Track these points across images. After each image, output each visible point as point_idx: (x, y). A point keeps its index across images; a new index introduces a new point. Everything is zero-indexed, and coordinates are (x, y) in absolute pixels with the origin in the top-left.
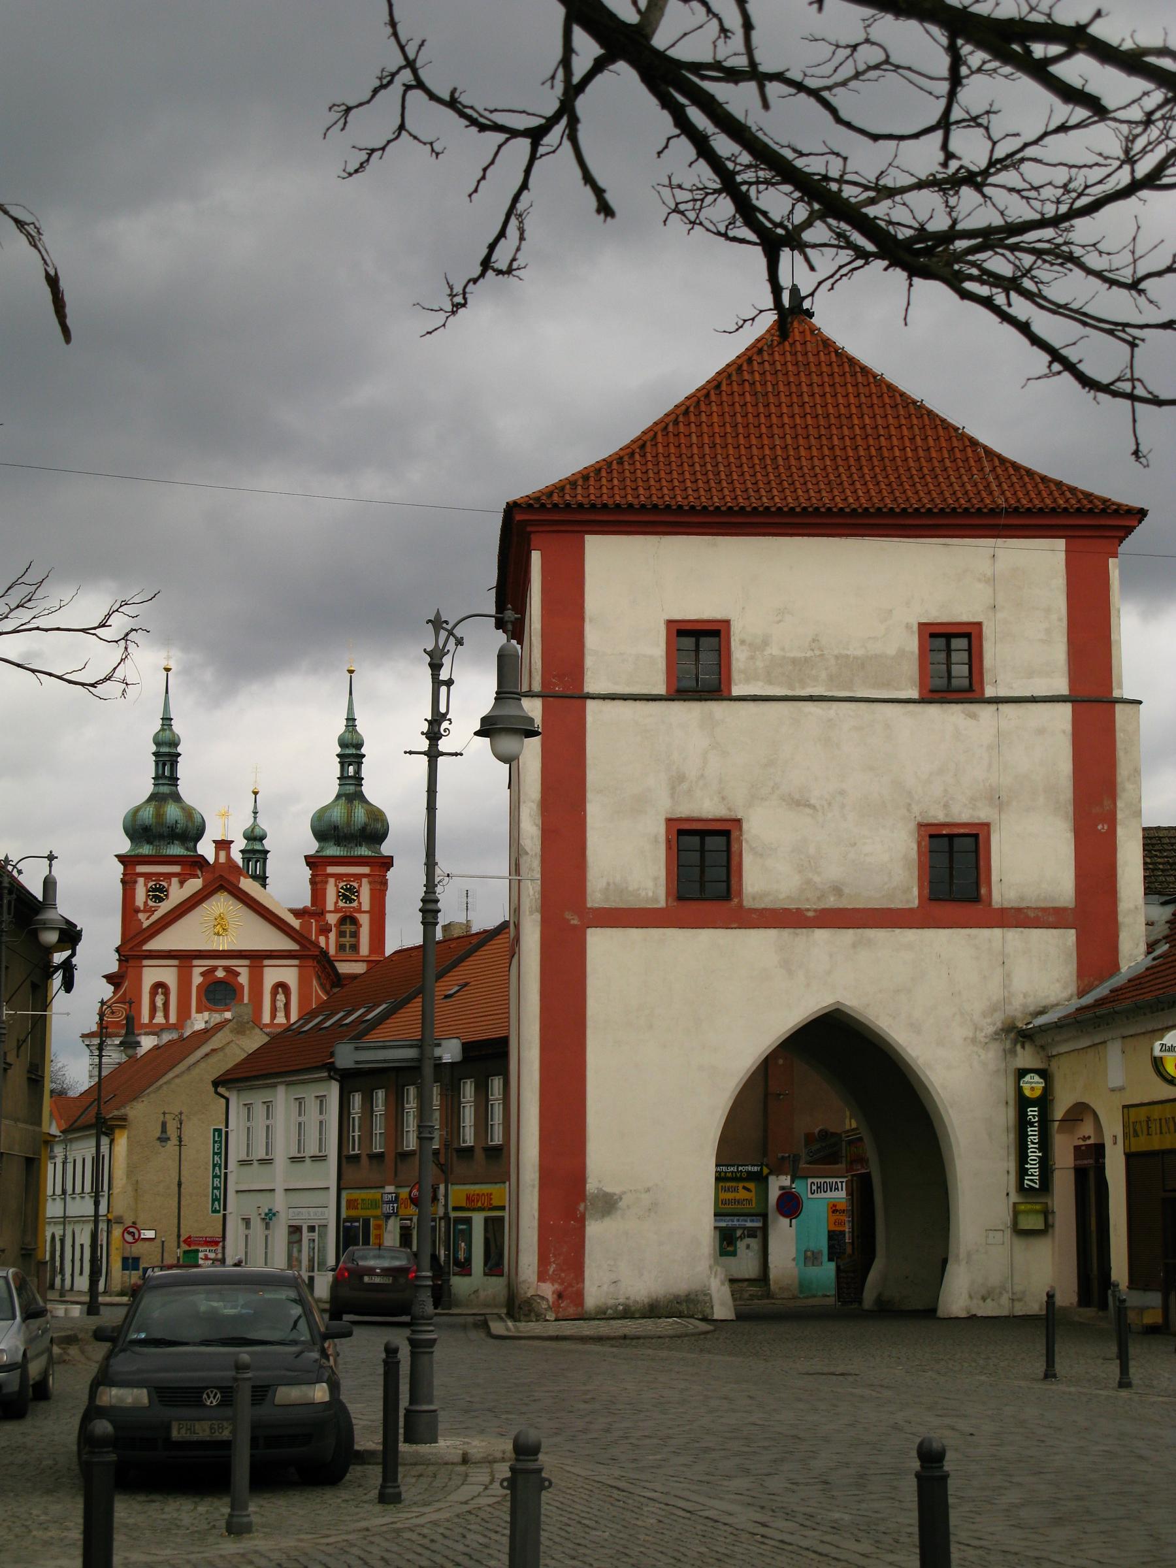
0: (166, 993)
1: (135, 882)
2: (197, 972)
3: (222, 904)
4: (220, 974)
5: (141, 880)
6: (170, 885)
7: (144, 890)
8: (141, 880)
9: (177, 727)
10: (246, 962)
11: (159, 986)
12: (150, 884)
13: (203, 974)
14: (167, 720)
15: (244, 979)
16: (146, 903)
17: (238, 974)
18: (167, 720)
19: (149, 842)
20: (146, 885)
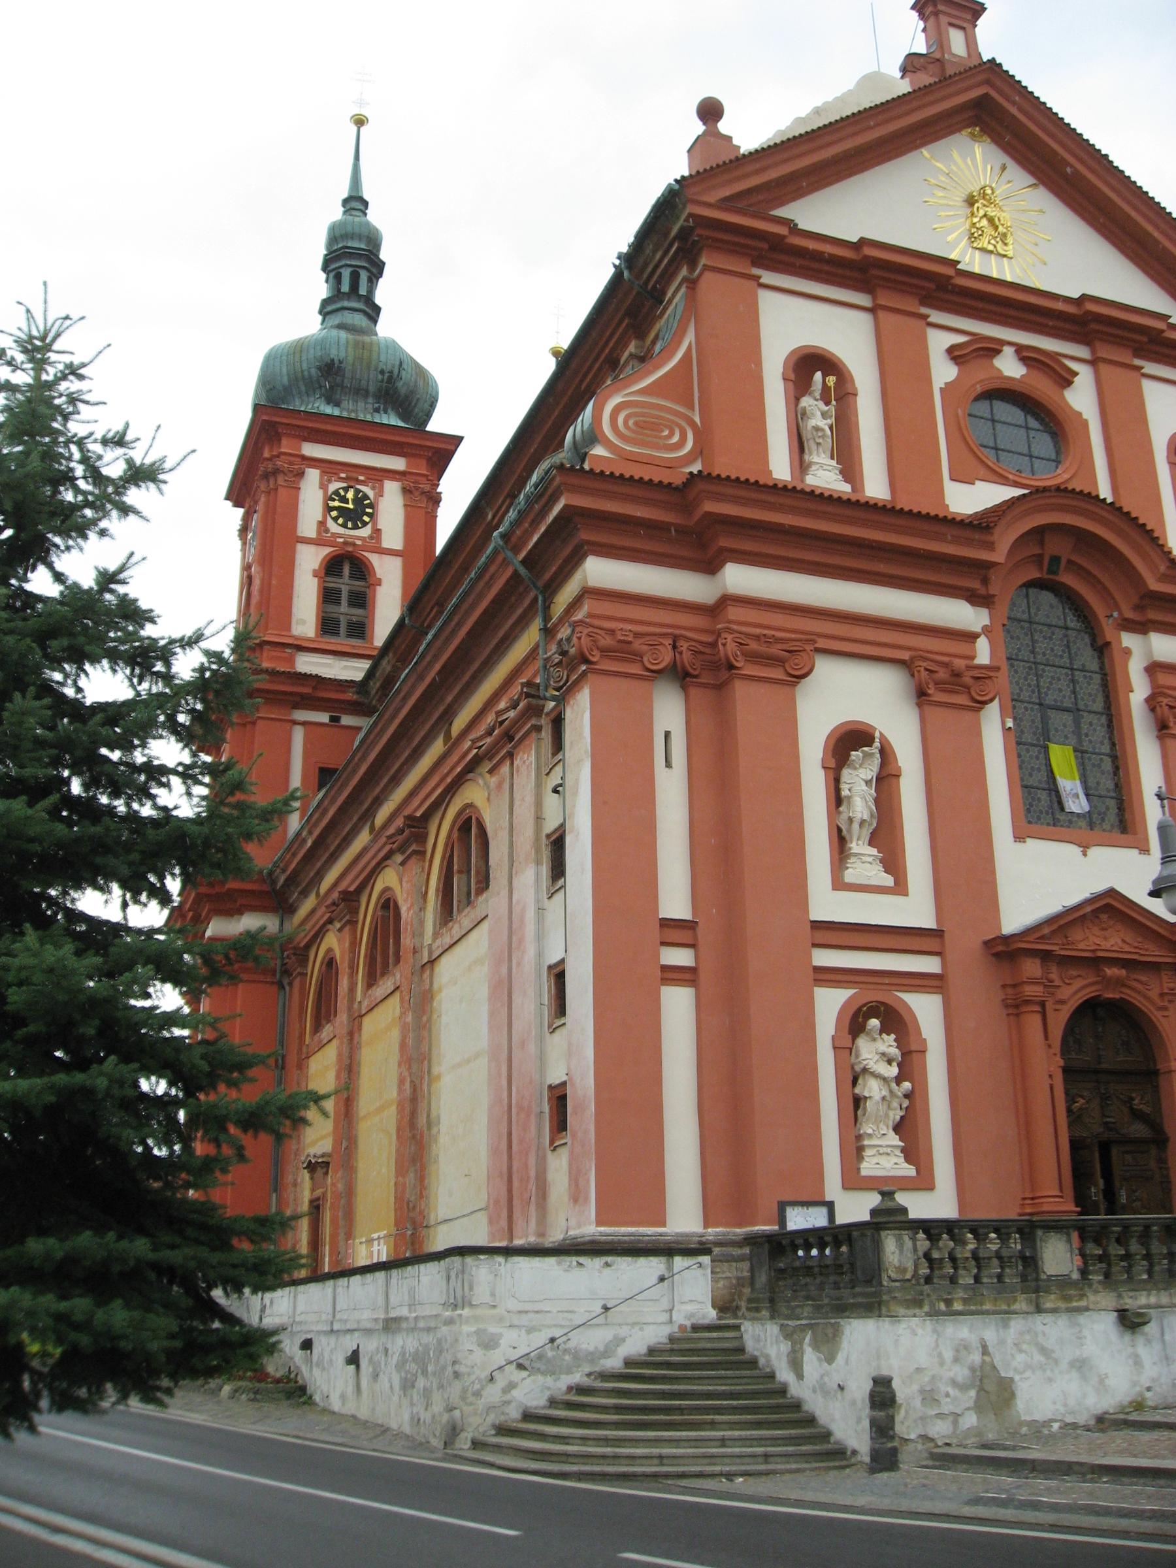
0: (842, 395)
1: (301, 474)
2: (939, 342)
3: (971, 161)
4: (1009, 367)
5: (313, 476)
6: (380, 494)
7: (320, 493)
8: (313, 476)
9: (374, 216)
10: (1083, 352)
11: (809, 365)
12: (334, 486)
13: (955, 354)
14: (355, 202)
15: (1082, 397)
16: (322, 524)
17: (1066, 379)
18: (355, 202)
19: (329, 401)
20: (323, 486)
